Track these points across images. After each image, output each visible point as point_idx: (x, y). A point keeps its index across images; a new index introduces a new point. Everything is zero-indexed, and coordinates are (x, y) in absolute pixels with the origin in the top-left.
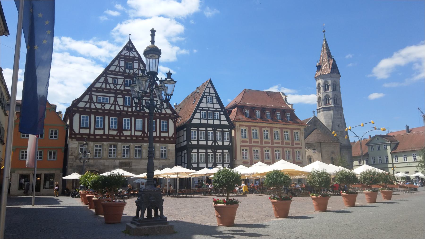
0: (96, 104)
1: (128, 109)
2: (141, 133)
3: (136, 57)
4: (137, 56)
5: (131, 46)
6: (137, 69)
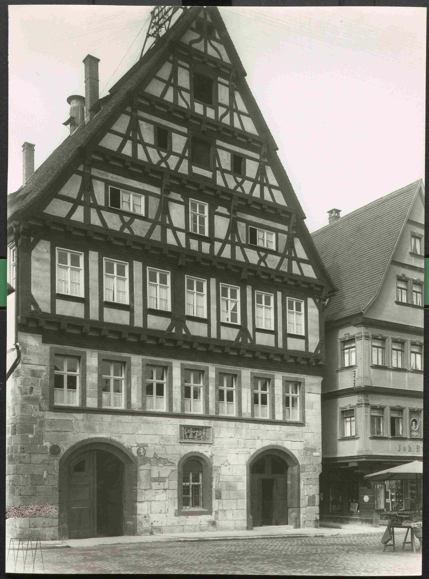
0: (104, 213)
1: (200, 246)
2: (236, 331)
3: (225, 66)
4: (226, 59)
5: (209, 19)
6: (224, 110)
